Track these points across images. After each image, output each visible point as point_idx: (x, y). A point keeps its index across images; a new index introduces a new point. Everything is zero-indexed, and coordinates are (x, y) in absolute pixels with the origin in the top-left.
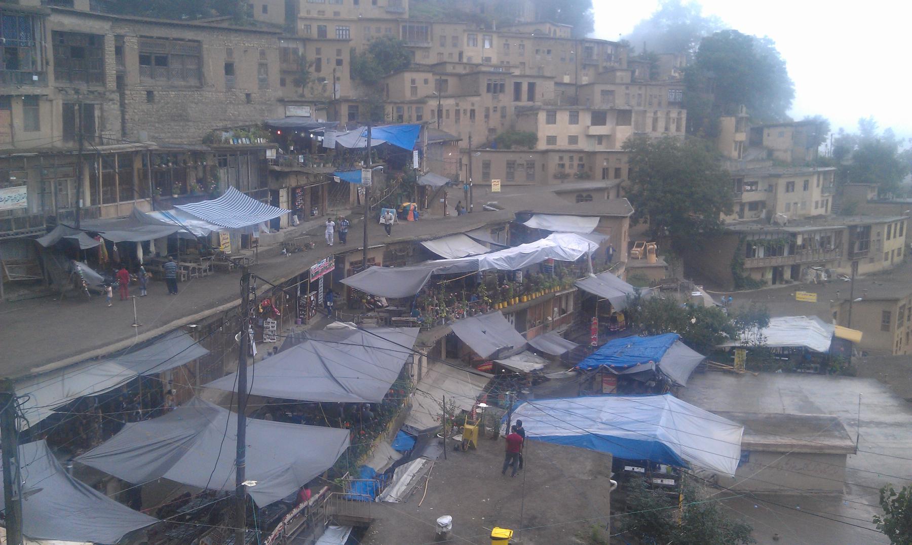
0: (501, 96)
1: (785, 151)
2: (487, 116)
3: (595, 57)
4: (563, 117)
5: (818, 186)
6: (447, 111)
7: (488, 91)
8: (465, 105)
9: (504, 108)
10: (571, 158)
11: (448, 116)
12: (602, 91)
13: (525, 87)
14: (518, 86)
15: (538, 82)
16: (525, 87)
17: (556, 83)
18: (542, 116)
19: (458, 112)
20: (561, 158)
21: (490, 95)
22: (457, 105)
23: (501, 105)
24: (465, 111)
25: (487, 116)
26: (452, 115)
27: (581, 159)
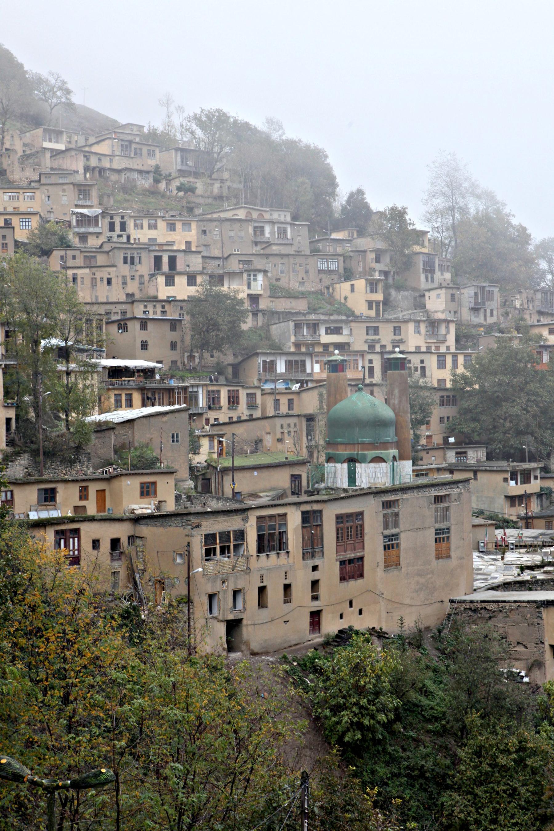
0: (138, 267)
1: (443, 312)
2: (125, 283)
3: (267, 234)
4: (181, 281)
5: (418, 332)
6: (82, 278)
7: (125, 262)
8: (103, 274)
9: (141, 277)
10: (155, 306)
11: (82, 283)
12: (240, 261)
13: (165, 260)
14: (158, 260)
15: (180, 256)
16: (165, 260)
17: (203, 257)
18: (161, 280)
19: (94, 280)
20: (145, 306)
21: (127, 266)
22: (94, 274)
23: (138, 274)
24: (102, 279)
25: (125, 283)
26: (88, 282)
27: (163, 307)
